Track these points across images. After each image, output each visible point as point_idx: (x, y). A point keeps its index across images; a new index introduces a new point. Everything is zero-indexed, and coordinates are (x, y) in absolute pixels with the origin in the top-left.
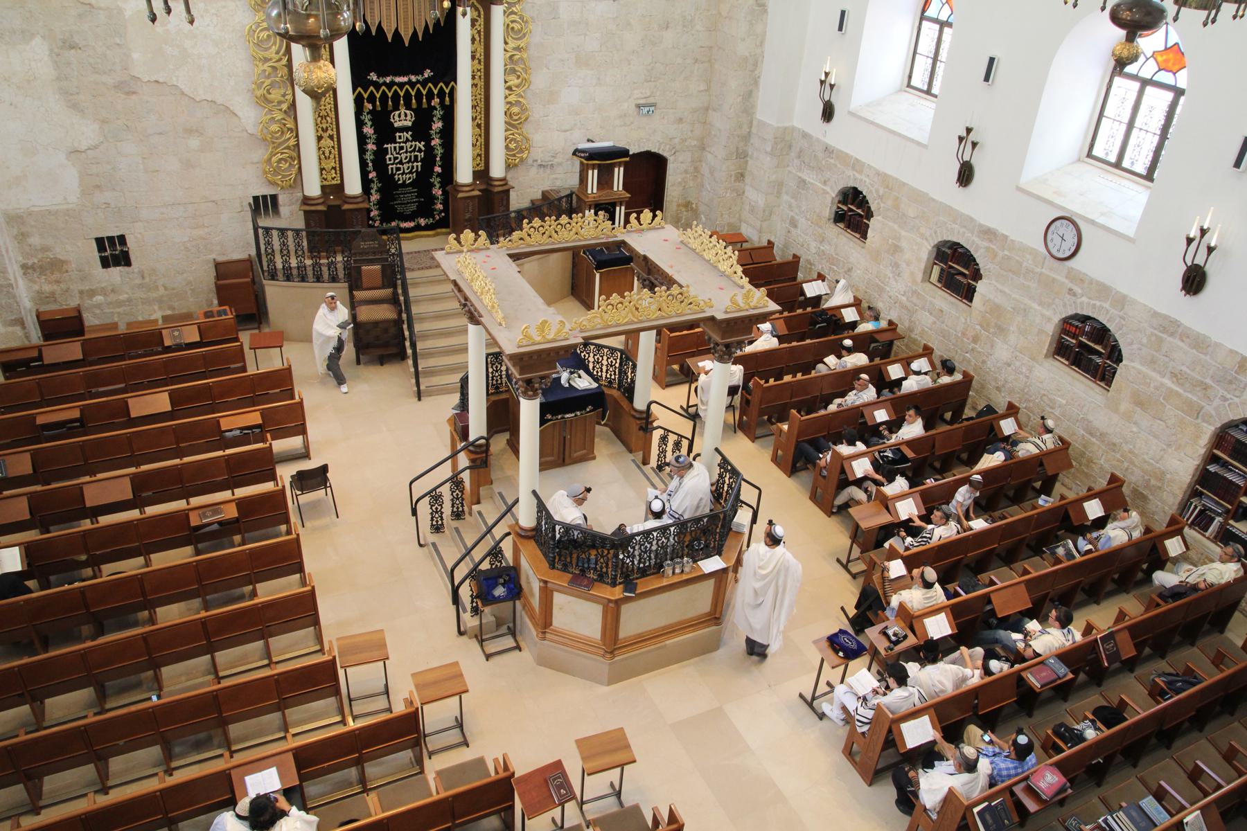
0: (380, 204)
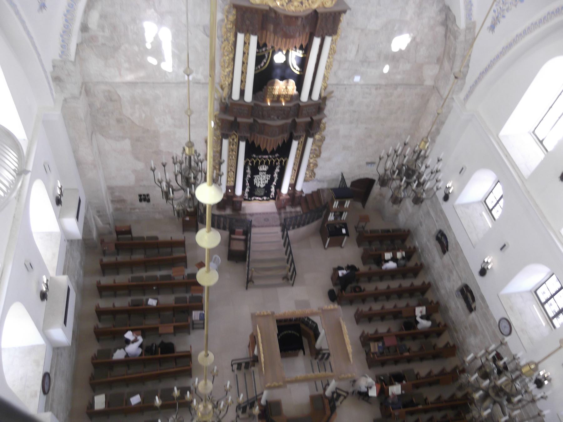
0: (248, 193)
